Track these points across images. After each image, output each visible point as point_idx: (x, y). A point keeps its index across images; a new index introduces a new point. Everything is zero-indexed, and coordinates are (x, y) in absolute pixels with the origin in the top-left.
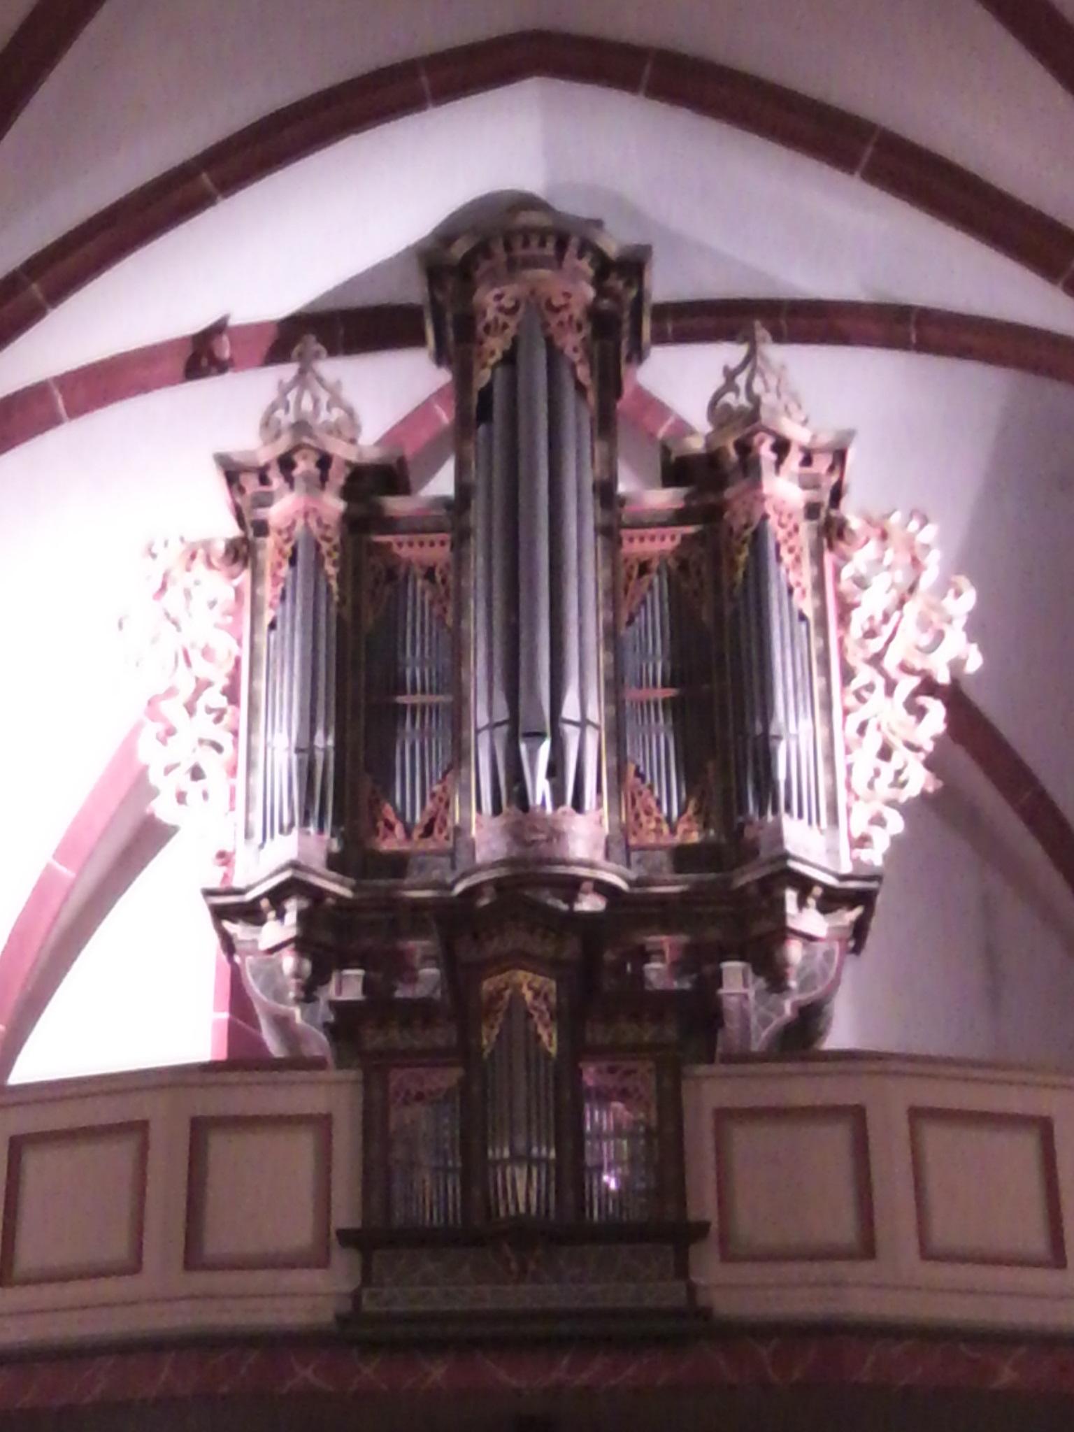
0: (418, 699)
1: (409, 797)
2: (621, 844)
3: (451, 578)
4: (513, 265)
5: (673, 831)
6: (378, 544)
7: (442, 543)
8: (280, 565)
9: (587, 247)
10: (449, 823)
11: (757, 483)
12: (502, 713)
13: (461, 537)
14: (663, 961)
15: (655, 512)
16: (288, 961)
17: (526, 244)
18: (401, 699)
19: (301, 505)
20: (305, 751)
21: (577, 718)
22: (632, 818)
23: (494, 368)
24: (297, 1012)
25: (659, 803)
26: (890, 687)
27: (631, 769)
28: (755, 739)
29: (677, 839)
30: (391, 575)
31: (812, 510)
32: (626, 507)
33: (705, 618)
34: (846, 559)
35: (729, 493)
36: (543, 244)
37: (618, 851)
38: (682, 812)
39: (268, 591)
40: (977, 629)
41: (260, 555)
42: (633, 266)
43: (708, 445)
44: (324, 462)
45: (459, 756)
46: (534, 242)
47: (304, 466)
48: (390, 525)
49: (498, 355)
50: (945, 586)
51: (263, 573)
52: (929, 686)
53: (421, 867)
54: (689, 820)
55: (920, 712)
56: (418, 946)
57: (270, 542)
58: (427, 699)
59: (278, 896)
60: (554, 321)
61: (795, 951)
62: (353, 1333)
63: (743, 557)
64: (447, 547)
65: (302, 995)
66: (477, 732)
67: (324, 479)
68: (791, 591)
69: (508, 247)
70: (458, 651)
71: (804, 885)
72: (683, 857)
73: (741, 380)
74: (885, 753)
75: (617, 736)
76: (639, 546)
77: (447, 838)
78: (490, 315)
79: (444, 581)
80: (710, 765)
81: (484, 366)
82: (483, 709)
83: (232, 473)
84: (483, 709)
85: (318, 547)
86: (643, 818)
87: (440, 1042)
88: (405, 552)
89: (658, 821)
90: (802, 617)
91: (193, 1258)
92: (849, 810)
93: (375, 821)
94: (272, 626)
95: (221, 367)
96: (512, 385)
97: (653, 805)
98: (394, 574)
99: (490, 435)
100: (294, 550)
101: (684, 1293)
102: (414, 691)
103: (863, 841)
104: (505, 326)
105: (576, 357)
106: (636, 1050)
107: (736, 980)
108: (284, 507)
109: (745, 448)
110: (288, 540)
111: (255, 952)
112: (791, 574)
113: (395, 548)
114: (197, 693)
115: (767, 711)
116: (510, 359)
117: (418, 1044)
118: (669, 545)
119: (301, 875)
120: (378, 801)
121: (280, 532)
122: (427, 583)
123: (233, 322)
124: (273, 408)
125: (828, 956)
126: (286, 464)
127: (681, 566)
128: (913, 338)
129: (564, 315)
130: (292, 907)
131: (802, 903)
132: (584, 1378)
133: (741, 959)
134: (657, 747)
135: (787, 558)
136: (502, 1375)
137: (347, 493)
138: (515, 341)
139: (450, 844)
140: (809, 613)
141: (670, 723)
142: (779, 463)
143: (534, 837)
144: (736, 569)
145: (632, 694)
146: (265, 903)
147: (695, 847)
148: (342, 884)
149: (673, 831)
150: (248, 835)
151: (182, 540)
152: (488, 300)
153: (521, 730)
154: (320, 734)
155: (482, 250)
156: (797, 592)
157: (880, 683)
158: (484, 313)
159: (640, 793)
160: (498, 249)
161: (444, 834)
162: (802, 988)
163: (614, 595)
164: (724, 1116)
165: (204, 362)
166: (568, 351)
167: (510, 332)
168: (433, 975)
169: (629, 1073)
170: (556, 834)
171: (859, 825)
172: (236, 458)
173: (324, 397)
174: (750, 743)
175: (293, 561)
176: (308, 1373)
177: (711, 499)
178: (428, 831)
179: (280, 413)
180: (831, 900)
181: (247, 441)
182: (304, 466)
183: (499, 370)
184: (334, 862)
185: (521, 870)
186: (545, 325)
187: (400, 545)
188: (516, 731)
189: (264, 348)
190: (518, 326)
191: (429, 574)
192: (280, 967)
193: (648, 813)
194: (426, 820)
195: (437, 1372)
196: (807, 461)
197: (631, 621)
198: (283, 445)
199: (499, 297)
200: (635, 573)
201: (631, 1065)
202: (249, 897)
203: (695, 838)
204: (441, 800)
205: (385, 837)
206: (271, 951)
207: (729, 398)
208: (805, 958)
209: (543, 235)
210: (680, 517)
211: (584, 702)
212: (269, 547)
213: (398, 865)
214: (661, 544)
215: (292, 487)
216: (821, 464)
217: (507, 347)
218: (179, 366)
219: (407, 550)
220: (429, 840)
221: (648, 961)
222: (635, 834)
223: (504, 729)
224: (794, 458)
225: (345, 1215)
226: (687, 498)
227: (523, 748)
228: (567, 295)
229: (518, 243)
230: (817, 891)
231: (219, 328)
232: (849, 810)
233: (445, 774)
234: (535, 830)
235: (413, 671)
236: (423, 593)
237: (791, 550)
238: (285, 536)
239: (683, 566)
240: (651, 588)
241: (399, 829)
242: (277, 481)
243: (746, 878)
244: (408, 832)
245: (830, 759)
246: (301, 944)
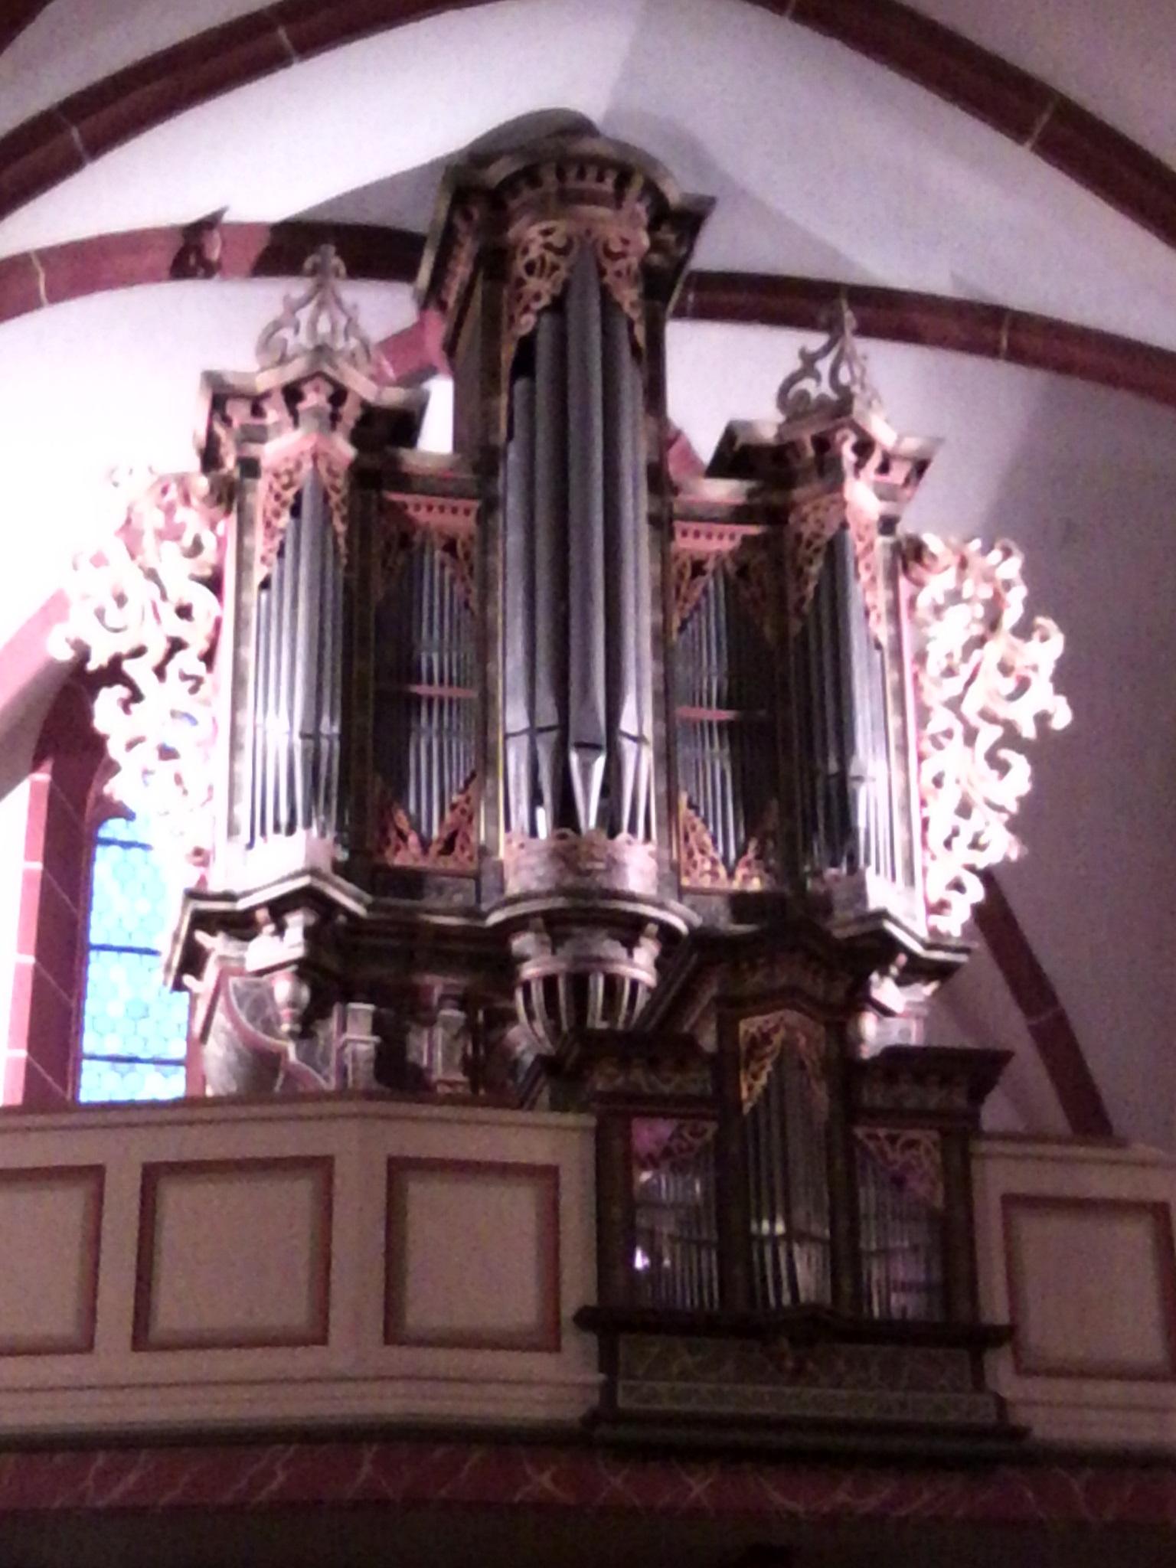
0: (435, 690)
1: (426, 807)
3: (475, 551)
4: (568, 199)
5: (731, 875)
6: (393, 504)
7: (467, 512)
8: (277, 515)
9: (653, 191)
10: (473, 839)
11: (837, 484)
12: (548, 713)
13: (490, 506)
15: (714, 506)
16: (283, 988)
17: (582, 175)
18: (416, 689)
19: (308, 446)
20: (311, 736)
21: (634, 732)
22: (684, 856)
23: (539, 313)
24: (291, 1048)
26: (970, 737)
27: (683, 799)
28: (828, 777)
29: (736, 885)
30: (405, 541)
32: (681, 497)
33: (768, 631)
34: (920, 584)
35: (798, 493)
36: (600, 179)
38: (741, 852)
39: (259, 542)
40: (1065, 679)
41: (250, 498)
42: (685, 221)
43: (779, 436)
44: (339, 396)
45: (486, 760)
46: (592, 173)
47: (314, 399)
48: (404, 481)
49: (545, 301)
50: (1024, 630)
51: (252, 522)
52: (1011, 737)
53: (440, 889)
54: (748, 864)
55: (1004, 769)
56: (436, 984)
57: (262, 484)
58: (446, 692)
59: (279, 908)
60: (611, 267)
62: (595, 1436)
63: (815, 569)
64: (472, 517)
65: (298, 1028)
66: (506, 736)
67: (335, 418)
68: (867, 614)
69: (561, 174)
70: (484, 642)
73: (824, 366)
74: (964, 810)
76: (689, 544)
77: (471, 858)
78: (534, 253)
79: (467, 556)
81: (527, 309)
83: (221, 396)
85: (326, 498)
86: (698, 856)
87: (694, 1089)
88: (422, 516)
89: (714, 862)
90: (878, 646)
91: (141, 1338)
92: (925, 871)
93: (384, 831)
94: (265, 585)
95: (208, 270)
96: (561, 339)
97: (708, 840)
98: (406, 538)
99: (532, 391)
100: (298, 496)
101: (992, 1409)
102: (430, 682)
103: (941, 907)
104: (555, 268)
105: (635, 315)
106: (921, 1117)
109: (824, 445)
110: (286, 487)
111: (241, 972)
112: (867, 592)
113: (411, 511)
114: (169, 655)
115: (845, 746)
116: (558, 306)
117: (667, 1089)
118: (727, 545)
119: (320, 884)
120: (389, 806)
121: (277, 475)
122: (447, 556)
123: (227, 218)
124: (277, 325)
126: (292, 394)
127: (740, 572)
128: (1004, 343)
129: (621, 264)
130: (296, 923)
132: (870, 1503)
135: (865, 576)
136: (777, 1498)
138: (566, 285)
139: (472, 867)
140: (884, 640)
141: (727, 750)
142: (859, 466)
143: (589, 866)
144: (806, 583)
145: (683, 711)
146: (262, 915)
147: (757, 896)
148: (358, 899)
149: (731, 875)
150: (232, 830)
151: (150, 469)
152: (531, 235)
153: (572, 739)
154: (326, 719)
155: (530, 175)
156: (873, 616)
157: (959, 729)
158: (526, 251)
159: (694, 828)
160: (549, 178)
161: (467, 853)
163: (665, 594)
164: (1010, 1201)
165: (192, 261)
166: (626, 307)
167: (562, 274)
168: (458, 1019)
169: (911, 1144)
171: (937, 891)
172: (231, 380)
173: (342, 322)
174: (820, 783)
175: (296, 511)
176: (617, 1482)
177: (775, 498)
178: (448, 846)
179: (287, 333)
181: (241, 362)
182: (314, 399)
183: (546, 320)
185: (581, 902)
186: (602, 273)
187: (417, 507)
189: (253, 254)
190: (571, 270)
191: (450, 547)
192: (271, 992)
193: (702, 852)
194: (445, 835)
195: (698, 1486)
196: (884, 468)
197: (682, 628)
198: (293, 371)
199: (546, 233)
200: (688, 573)
201: (914, 1134)
202: (242, 905)
203: (755, 885)
204: (463, 811)
205: (398, 849)
206: (260, 973)
207: (808, 385)
208: (879, 1034)
209: (603, 165)
210: (740, 514)
211: (637, 716)
212: (260, 494)
214: (718, 544)
215: (296, 424)
216: (898, 474)
217: (557, 291)
218: (165, 259)
222: (688, 873)
223: (553, 736)
224: (875, 460)
225: (578, 1289)
226: (751, 494)
227: (574, 759)
228: (626, 242)
229: (572, 173)
231: (208, 224)
232: (925, 871)
233: (467, 783)
234: (592, 858)
235: (431, 657)
236: (442, 566)
237: (868, 567)
238: (285, 479)
239: (743, 571)
240: (705, 592)
241: (413, 839)
242: (274, 414)
244: (425, 844)
245: (906, 809)
246: (304, 969)
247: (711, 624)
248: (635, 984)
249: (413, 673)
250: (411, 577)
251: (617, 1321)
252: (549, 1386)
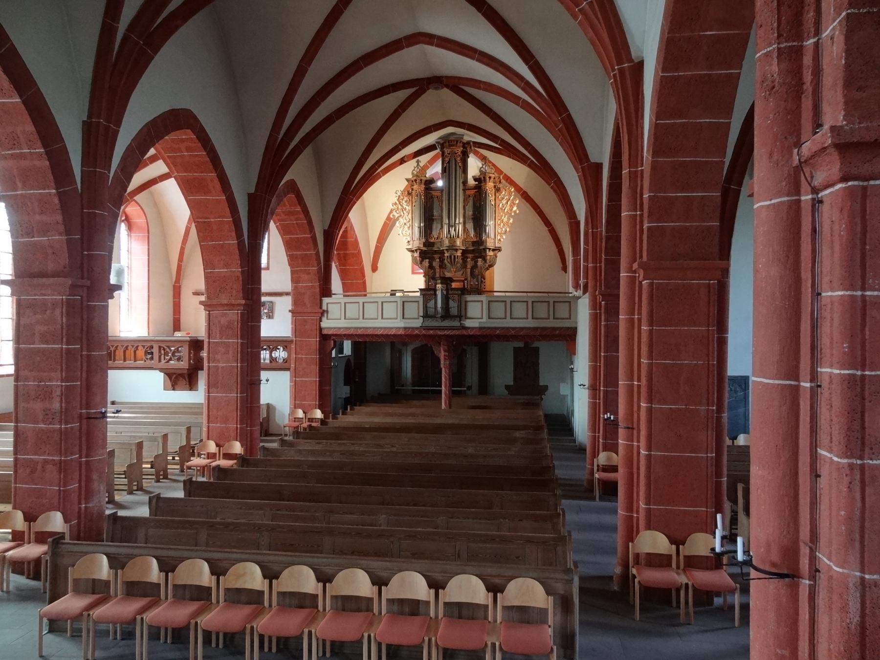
1: (435, 233)
2: (464, 241)
4: (450, 146)
20: (420, 228)
31: (495, 187)
48: (431, 189)
61: (488, 257)
72: (474, 243)
75: (464, 223)
82: (446, 221)
83: (407, 180)
84: (446, 221)
95: (405, 162)
107: (480, 262)
108: (415, 187)
112: (491, 198)
116: (449, 162)
134: (470, 226)
137: (425, 184)
170: (455, 242)
180: (493, 250)
181: (410, 176)
184: (425, 245)
188: (449, 226)
195: (431, 332)
213: (433, 244)
219: (433, 193)
235: (435, 213)
243: (481, 248)
247: (471, 203)
249: (433, 215)
250: (433, 201)
251: (426, 316)
252: (418, 323)
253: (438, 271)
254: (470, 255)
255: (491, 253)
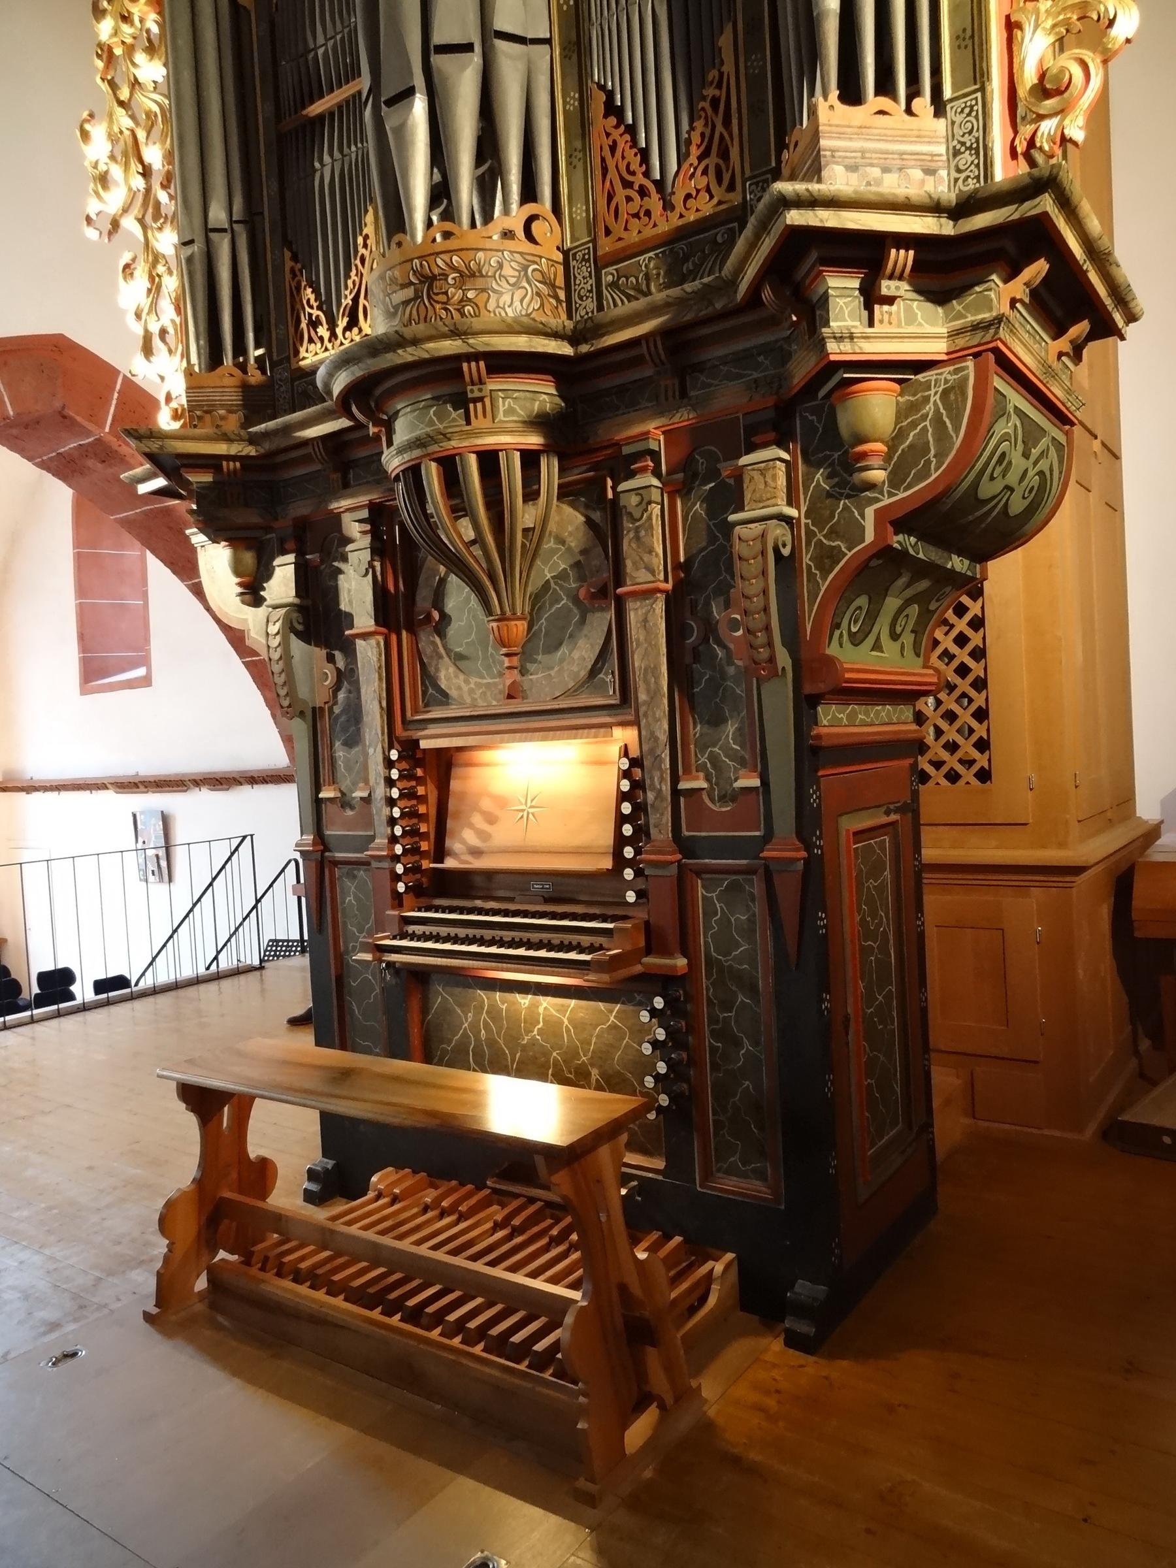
14: (657, 473)
25: (645, 154)
29: (675, 221)
37: (583, 274)
71: (865, 253)
80: (725, 41)
86: (621, 193)
125: (954, 394)
131: (871, 298)
133: (781, 444)
162: (896, 480)
180: (944, 269)
193: (627, 184)
208: (902, 413)
220: (355, 330)
221: (631, 475)
230: (903, 258)
248: (489, 460)
253: (369, 653)
254: (653, 430)
255: (912, 327)
